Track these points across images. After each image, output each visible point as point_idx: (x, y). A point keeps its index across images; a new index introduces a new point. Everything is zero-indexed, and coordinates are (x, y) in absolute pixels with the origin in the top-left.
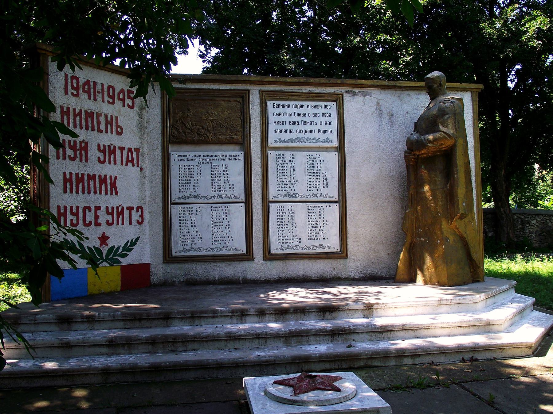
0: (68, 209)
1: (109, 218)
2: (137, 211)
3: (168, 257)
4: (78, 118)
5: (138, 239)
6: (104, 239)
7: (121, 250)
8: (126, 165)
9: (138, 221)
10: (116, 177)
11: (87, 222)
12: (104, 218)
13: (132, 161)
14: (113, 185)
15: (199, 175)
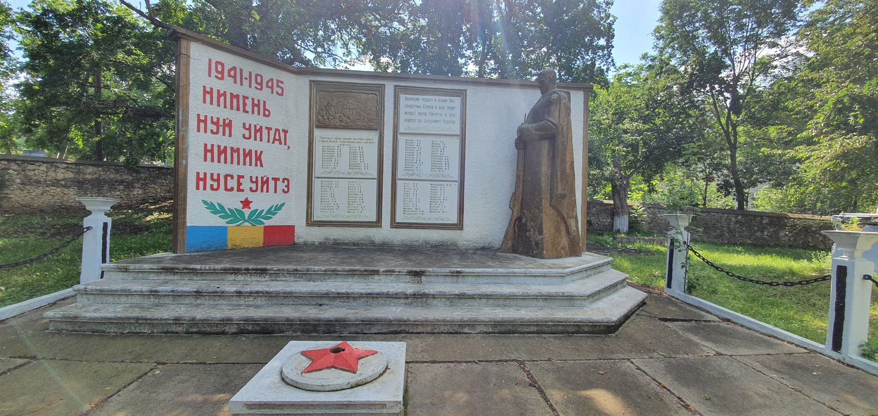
0: (209, 176)
1: (254, 186)
2: (283, 182)
3: (311, 222)
4: (222, 98)
5: (283, 204)
6: (246, 203)
7: (264, 213)
8: (273, 143)
9: (284, 191)
10: (261, 152)
11: (229, 188)
12: (246, 184)
13: (279, 140)
14: (258, 158)
15: (340, 154)
